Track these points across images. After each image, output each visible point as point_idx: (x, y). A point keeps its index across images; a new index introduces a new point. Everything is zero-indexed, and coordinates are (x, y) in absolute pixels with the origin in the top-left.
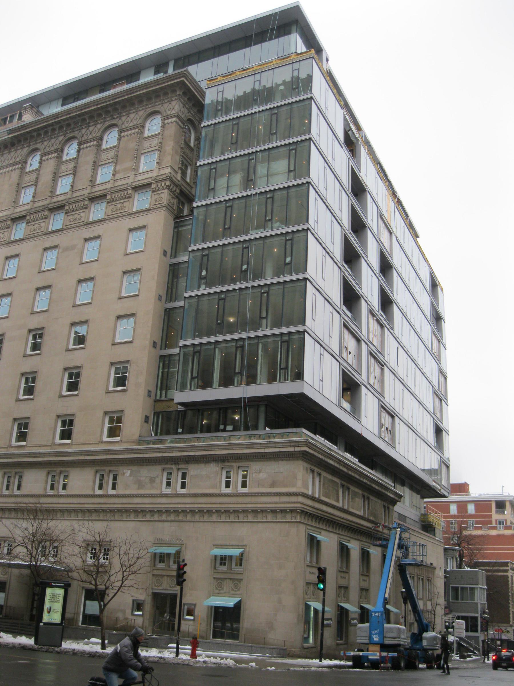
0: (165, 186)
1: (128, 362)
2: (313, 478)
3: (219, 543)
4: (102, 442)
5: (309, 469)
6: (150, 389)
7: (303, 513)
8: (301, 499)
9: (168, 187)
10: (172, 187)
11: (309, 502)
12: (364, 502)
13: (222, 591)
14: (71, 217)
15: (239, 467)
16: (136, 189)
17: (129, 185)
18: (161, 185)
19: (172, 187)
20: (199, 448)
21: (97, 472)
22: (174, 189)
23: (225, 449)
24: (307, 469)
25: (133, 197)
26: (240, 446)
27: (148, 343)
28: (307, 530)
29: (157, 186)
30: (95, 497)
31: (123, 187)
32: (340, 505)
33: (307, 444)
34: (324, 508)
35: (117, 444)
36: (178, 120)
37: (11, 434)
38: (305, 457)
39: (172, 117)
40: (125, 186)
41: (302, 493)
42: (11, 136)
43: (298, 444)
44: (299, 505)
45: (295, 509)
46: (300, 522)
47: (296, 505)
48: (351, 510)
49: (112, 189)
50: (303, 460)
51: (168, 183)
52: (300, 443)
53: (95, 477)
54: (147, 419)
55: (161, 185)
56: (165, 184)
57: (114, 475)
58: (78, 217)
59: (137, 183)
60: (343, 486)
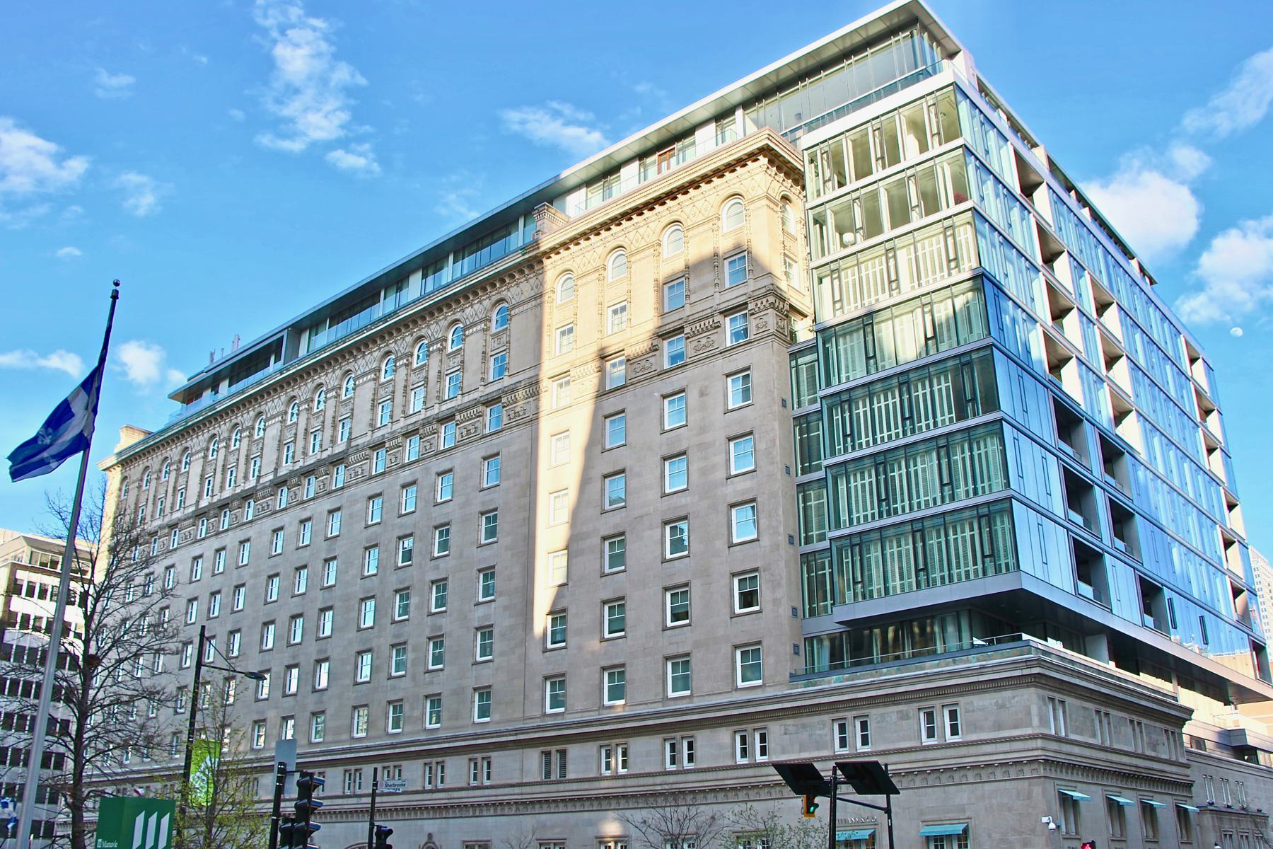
0: (768, 305)
1: (756, 570)
2: (1054, 709)
5: (1047, 699)
6: (795, 605)
8: (1039, 743)
9: (772, 306)
11: (1054, 746)
12: (1134, 730)
15: (943, 706)
16: (725, 314)
17: (713, 309)
18: (762, 303)
20: (881, 685)
22: (781, 306)
23: (920, 683)
24: (1044, 700)
25: (723, 326)
26: (941, 676)
27: (783, 539)
28: (1057, 787)
29: (757, 305)
30: (737, 769)
31: (705, 313)
32: (1097, 741)
34: (1076, 750)
36: (768, 202)
37: (601, 689)
38: (1039, 680)
39: (760, 199)
40: (709, 311)
41: (1041, 734)
42: (526, 256)
44: (1039, 752)
45: (1035, 758)
46: (1045, 777)
47: (1036, 753)
48: (1116, 746)
49: (691, 318)
50: (1036, 686)
51: (772, 299)
52: (1028, 664)
55: (762, 303)
56: (767, 301)
57: (761, 734)
58: (647, 365)
59: (726, 304)
60: (1098, 712)
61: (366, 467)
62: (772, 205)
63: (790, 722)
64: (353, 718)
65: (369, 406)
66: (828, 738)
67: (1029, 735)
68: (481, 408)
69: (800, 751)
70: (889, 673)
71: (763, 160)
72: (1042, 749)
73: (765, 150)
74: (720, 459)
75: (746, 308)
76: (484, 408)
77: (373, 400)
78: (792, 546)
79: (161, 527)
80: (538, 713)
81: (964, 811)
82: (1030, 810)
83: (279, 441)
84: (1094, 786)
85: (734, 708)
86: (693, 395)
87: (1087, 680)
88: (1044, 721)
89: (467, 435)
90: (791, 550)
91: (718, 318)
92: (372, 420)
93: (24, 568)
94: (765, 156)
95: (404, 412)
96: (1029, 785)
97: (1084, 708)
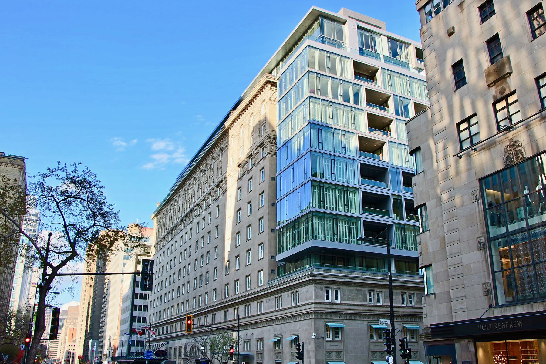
3: (291, 334)
4: (258, 287)
7: (316, 313)
8: (313, 306)
9: (269, 142)
10: (272, 141)
22: (274, 141)
23: (289, 283)
33: (312, 275)
36: (271, 102)
38: (314, 282)
43: (309, 275)
44: (313, 309)
46: (315, 318)
50: (314, 284)
53: (258, 305)
54: (272, 272)
61: (197, 213)
63: (267, 298)
64: (193, 302)
66: (274, 304)
67: (311, 302)
68: (216, 189)
70: (286, 279)
71: (269, 86)
73: (268, 82)
74: (257, 202)
75: (263, 146)
76: (217, 188)
77: (198, 188)
79: (162, 239)
80: (223, 298)
81: (298, 331)
84: (359, 321)
85: (255, 294)
86: (253, 178)
87: (355, 279)
88: (317, 297)
90: (273, 235)
91: (259, 149)
93: (141, 255)
94: (269, 84)
95: (203, 191)
97: (358, 290)
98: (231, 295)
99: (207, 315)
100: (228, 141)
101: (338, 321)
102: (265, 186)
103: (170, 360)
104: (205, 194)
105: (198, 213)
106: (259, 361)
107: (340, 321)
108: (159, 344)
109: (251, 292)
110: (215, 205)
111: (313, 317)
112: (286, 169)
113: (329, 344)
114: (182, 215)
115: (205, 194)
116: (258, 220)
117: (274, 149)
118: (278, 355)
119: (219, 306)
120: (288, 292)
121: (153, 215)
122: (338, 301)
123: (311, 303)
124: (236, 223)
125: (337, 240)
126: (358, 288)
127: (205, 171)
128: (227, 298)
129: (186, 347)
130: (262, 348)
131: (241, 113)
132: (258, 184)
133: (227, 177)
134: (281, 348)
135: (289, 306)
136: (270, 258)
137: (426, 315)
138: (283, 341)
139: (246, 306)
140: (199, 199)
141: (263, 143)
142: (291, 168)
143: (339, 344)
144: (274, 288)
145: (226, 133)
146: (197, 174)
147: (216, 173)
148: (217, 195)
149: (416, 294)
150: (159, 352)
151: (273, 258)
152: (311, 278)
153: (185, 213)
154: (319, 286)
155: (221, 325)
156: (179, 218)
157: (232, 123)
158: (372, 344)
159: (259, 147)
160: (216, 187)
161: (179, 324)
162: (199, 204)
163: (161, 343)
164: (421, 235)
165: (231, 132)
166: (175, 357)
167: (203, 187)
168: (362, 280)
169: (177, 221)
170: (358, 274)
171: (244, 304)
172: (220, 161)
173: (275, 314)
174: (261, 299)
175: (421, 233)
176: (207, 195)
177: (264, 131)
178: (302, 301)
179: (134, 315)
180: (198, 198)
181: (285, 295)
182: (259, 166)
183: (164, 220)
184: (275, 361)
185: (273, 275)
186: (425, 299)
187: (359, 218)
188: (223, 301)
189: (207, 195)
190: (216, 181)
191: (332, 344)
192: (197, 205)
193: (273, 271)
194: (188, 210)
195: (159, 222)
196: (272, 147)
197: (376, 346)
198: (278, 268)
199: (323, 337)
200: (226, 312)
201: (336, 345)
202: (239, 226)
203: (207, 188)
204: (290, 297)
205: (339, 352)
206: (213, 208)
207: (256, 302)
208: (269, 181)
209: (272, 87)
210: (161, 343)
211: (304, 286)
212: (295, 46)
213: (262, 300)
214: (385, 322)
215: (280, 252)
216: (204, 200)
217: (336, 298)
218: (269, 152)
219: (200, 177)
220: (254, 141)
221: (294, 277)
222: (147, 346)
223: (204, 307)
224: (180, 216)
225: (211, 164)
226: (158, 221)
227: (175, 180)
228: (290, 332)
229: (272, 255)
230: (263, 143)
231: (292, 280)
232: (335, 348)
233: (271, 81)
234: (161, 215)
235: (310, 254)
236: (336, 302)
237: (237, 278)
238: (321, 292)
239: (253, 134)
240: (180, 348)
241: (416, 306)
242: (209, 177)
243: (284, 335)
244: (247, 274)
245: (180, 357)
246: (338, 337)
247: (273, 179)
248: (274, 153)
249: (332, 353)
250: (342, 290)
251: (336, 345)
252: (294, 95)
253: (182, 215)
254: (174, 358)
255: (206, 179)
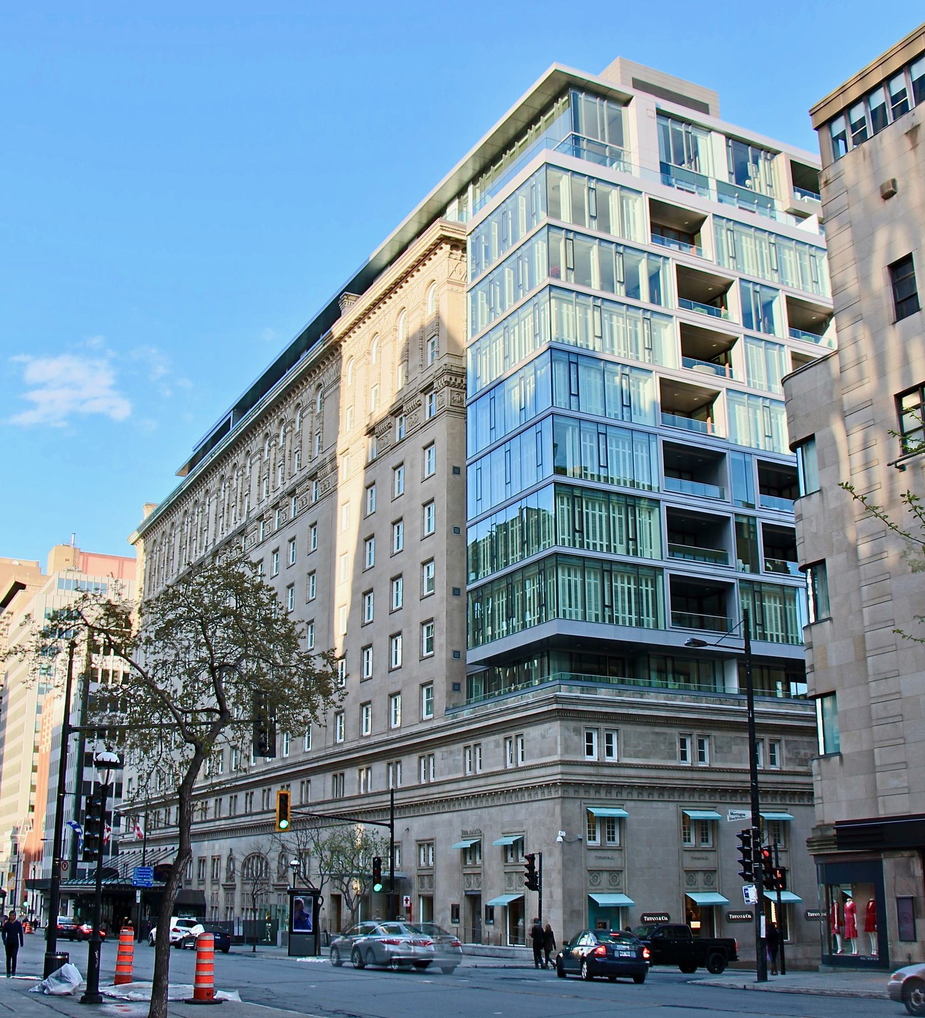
3: (506, 830)
4: (422, 721)
7: (565, 784)
8: (559, 769)
9: (448, 384)
10: (453, 380)
13: (512, 888)
14: (381, 442)
19: (453, 380)
21: (421, 758)
22: (459, 381)
23: (499, 716)
33: (557, 699)
35: (431, 722)
36: (450, 286)
38: (561, 715)
42: (326, 346)
43: (549, 701)
44: (559, 777)
51: (446, 378)
53: (420, 764)
54: (456, 687)
61: (256, 536)
62: (455, 288)
63: (444, 749)
65: (257, 484)
66: (462, 763)
67: (554, 762)
68: (308, 483)
69: (449, 774)
70: (491, 707)
71: (446, 247)
72: (562, 773)
73: (443, 239)
74: (418, 523)
75: (432, 390)
77: (259, 477)
78: (458, 597)
80: (331, 744)
81: (522, 825)
82: (554, 826)
83: (216, 515)
84: (660, 803)
87: (650, 709)
88: (566, 749)
89: (303, 505)
90: (456, 601)
91: (420, 397)
92: (259, 495)
94: (447, 244)
95: (273, 487)
96: (554, 804)
97: (657, 733)
98: (350, 738)
99: (288, 783)
100: (339, 370)
101: (613, 802)
102: (440, 488)
103: (188, 887)
104: (278, 493)
105: (258, 537)
106: (426, 893)
107: (617, 802)
108: (156, 848)
109: (404, 732)
110: (308, 519)
111: (560, 794)
112: (490, 452)
113: (594, 854)
114: (214, 540)
115: (278, 493)
116: (419, 565)
117: (458, 398)
118: (473, 879)
119: (320, 763)
120: (497, 737)
121: (137, 535)
122: (613, 759)
123: (554, 764)
124: (361, 569)
125: (611, 621)
126: (657, 729)
127: (278, 436)
128: (341, 744)
129: (231, 859)
130: (431, 863)
131: (375, 305)
132: (420, 480)
133: (338, 456)
134: (479, 862)
135: (500, 768)
136: (451, 655)
137: (822, 798)
138: (486, 848)
139: (389, 764)
140: (262, 505)
141: (432, 383)
142: (502, 449)
143: (616, 855)
144: (463, 726)
145: (334, 350)
146: (254, 443)
147: (306, 445)
148: (311, 497)
149: (786, 741)
150: (162, 870)
151: (457, 654)
152: (554, 707)
153: (225, 535)
154: (572, 724)
155: (326, 807)
156: (206, 547)
157: (350, 329)
158: (687, 856)
159: (421, 392)
160: (310, 479)
161: (212, 802)
162: (263, 515)
163: (163, 848)
164: (813, 628)
165: (346, 348)
166: (202, 881)
167: (271, 475)
168: (668, 711)
169: (203, 553)
170: (656, 698)
171: (385, 759)
172: (318, 416)
173: (465, 785)
174: (429, 749)
175: (813, 624)
176: (284, 497)
177: (433, 355)
178: (532, 756)
179: (86, 778)
180: (260, 501)
181: (489, 742)
182: (423, 438)
183: (165, 549)
184: (466, 891)
185: (456, 694)
186: (819, 765)
187: (661, 569)
188: (331, 751)
189: (284, 497)
190: (308, 465)
191: (600, 854)
192: (257, 519)
193: (456, 687)
194: (233, 527)
195: (150, 554)
196: (455, 395)
197: (696, 858)
198: (470, 678)
199: (581, 840)
200: (339, 779)
201: (609, 858)
202: (369, 576)
203: (283, 478)
204: (502, 749)
205: (615, 873)
206: (300, 529)
207: (415, 757)
208: (448, 475)
209: (454, 251)
210: (163, 848)
211: (536, 725)
212: (508, 151)
213: (430, 752)
214: (741, 815)
215: (476, 644)
216: (275, 507)
217: (609, 752)
218: (447, 405)
219: (263, 450)
220: (407, 377)
221: (512, 702)
222: (123, 853)
223: (280, 764)
224: (210, 541)
225: (294, 422)
226: (149, 549)
227: (192, 449)
228: (503, 827)
229: (456, 648)
230: (432, 383)
231: (508, 709)
232: (606, 864)
233: (450, 237)
234: (156, 535)
235: (548, 652)
236: (609, 759)
237: (367, 699)
238: (576, 738)
239: (406, 357)
240: (216, 860)
241: (784, 769)
242: (287, 453)
243: (487, 834)
244: (393, 689)
245: (215, 881)
246: (613, 839)
247: (456, 471)
248: (459, 410)
249: (599, 874)
250: (621, 732)
251: (609, 858)
252: (509, 276)
253: (214, 540)
254: (199, 884)
255: (280, 457)
